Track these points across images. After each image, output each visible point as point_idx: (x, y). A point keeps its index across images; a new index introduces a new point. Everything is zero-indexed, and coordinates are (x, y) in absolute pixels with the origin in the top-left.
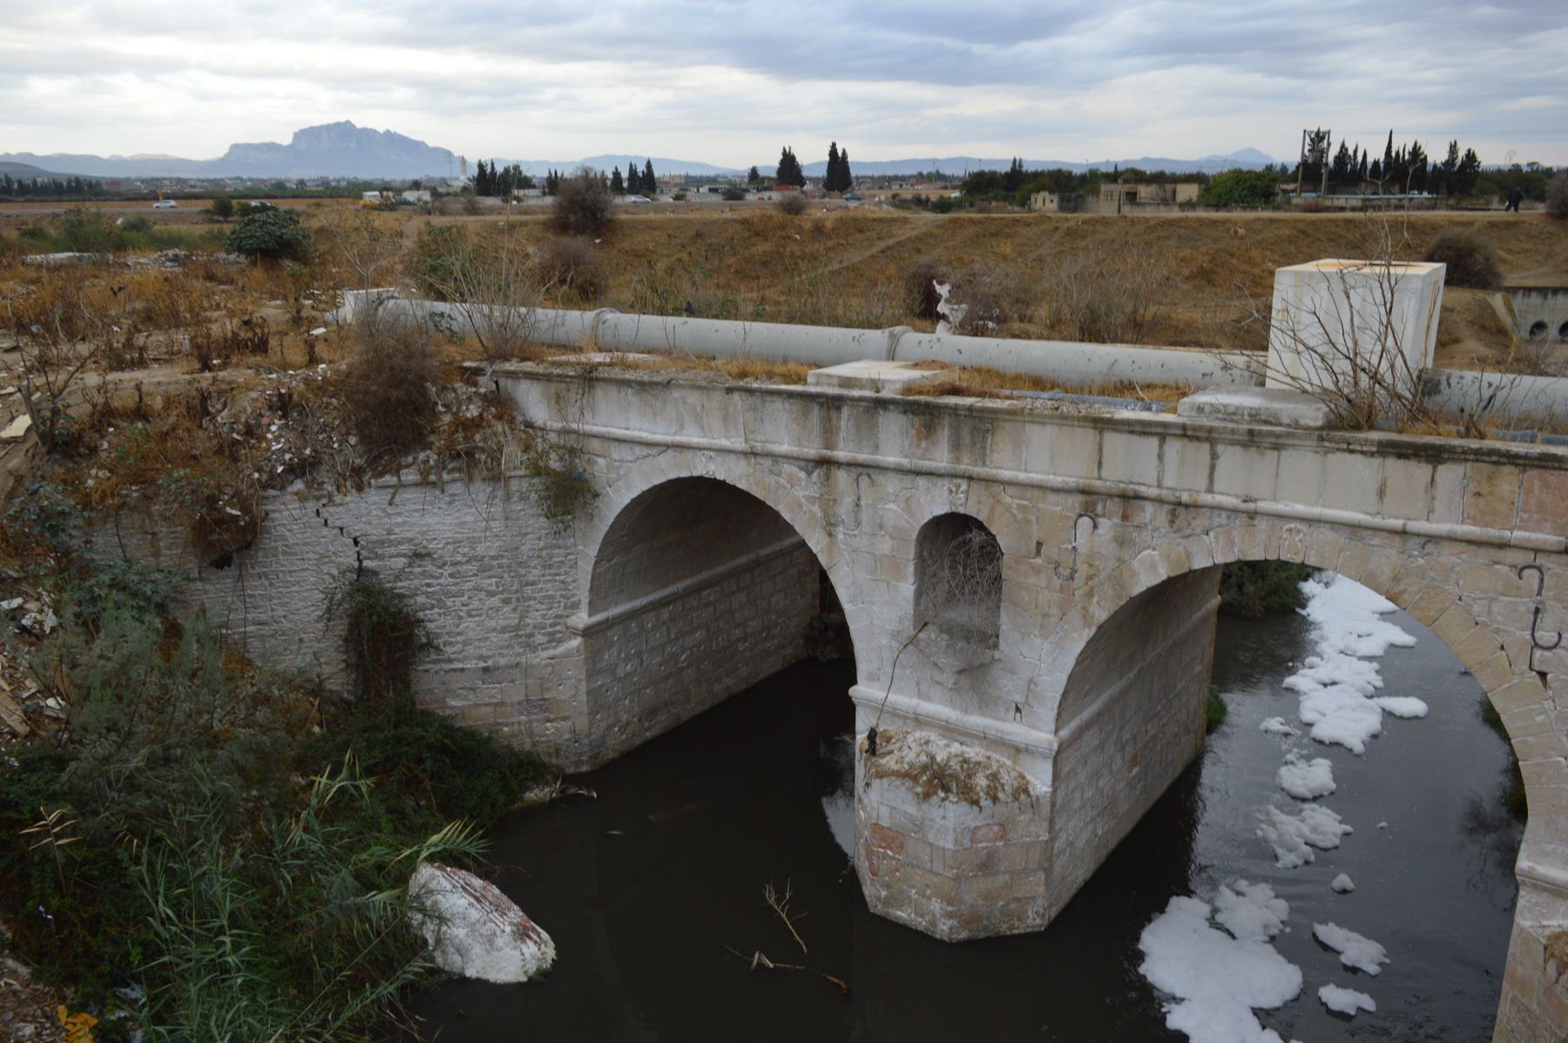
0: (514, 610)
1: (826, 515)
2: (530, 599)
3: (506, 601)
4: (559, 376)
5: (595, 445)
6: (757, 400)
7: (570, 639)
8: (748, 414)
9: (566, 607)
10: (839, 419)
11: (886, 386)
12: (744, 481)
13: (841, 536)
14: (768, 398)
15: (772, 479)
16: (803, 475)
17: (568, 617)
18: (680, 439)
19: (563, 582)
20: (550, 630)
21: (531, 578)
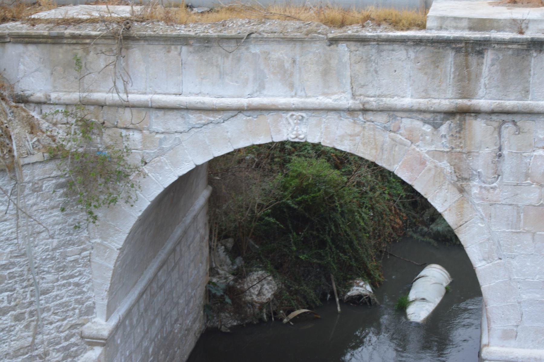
0: (27, 327)
1: (457, 169)
2: (43, 310)
3: (18, 318)
4: (73, 37)
5: (127, 116)
6: (371, 50)
7: (85, 350)
8: (357, 67)
9: (81, 315)
10: (480, 64)
11: (531, 26)
12: (346, 142)
13: (475, 191)
14: (387, 47)
15: (387, 137)
16: (428, 128)
17: (82, 325)
18: (257, 101)
19: (77, 285)
20: (65, 344)
21: (44, 285)
